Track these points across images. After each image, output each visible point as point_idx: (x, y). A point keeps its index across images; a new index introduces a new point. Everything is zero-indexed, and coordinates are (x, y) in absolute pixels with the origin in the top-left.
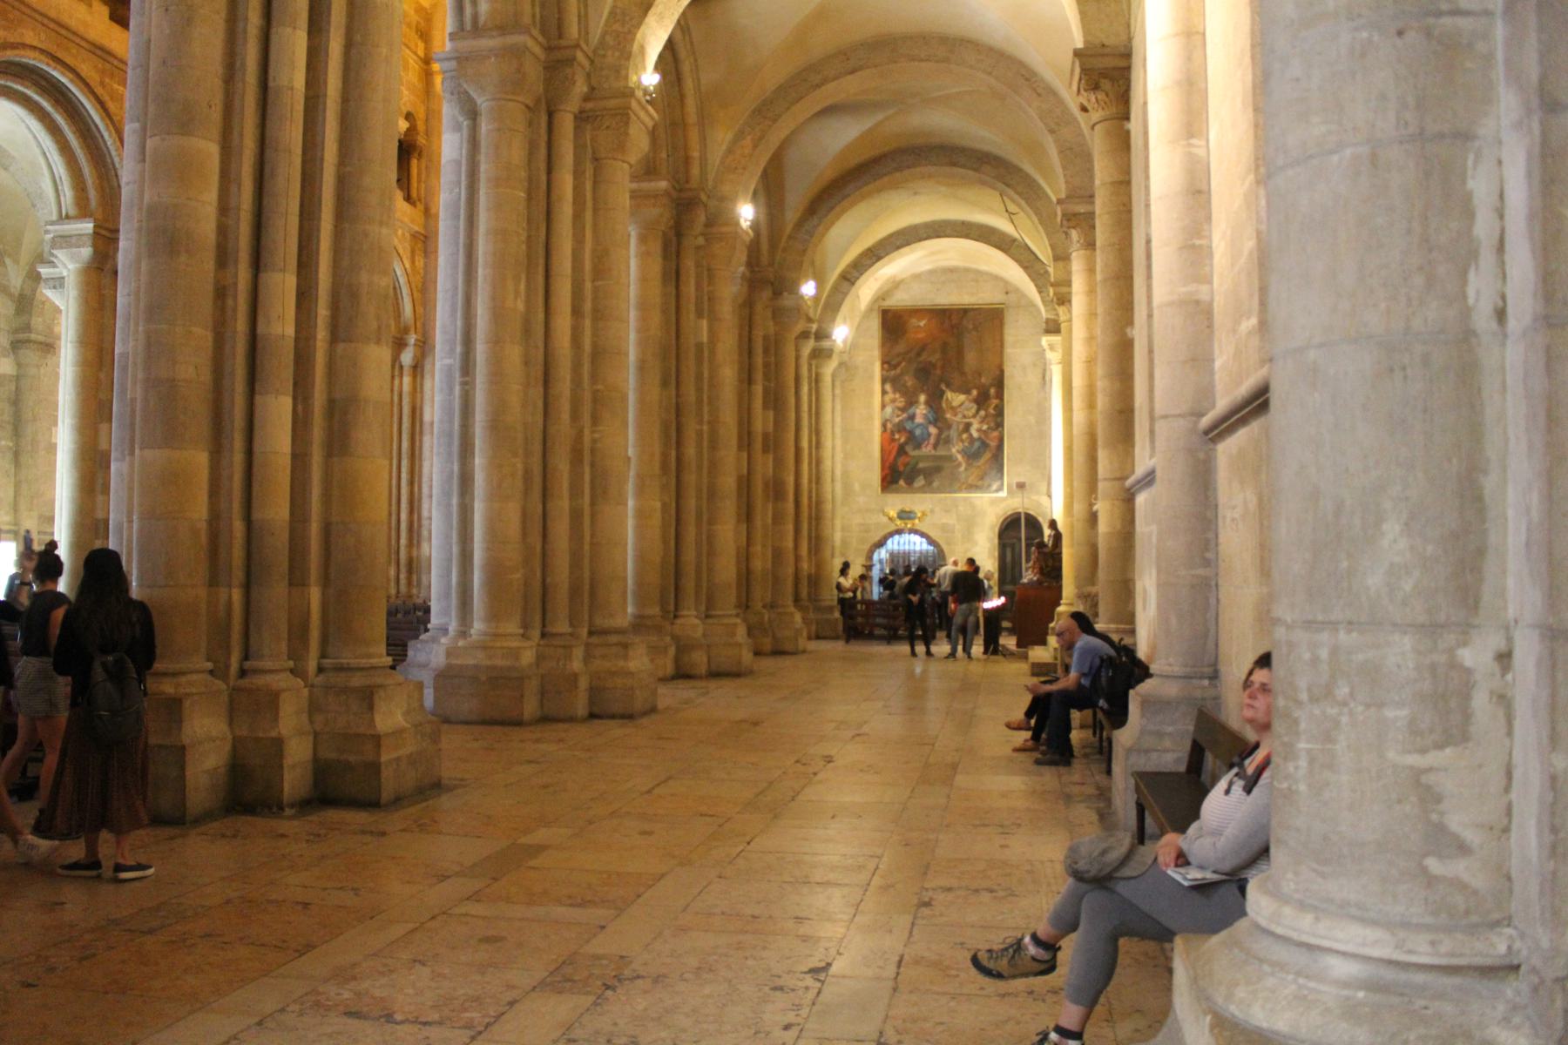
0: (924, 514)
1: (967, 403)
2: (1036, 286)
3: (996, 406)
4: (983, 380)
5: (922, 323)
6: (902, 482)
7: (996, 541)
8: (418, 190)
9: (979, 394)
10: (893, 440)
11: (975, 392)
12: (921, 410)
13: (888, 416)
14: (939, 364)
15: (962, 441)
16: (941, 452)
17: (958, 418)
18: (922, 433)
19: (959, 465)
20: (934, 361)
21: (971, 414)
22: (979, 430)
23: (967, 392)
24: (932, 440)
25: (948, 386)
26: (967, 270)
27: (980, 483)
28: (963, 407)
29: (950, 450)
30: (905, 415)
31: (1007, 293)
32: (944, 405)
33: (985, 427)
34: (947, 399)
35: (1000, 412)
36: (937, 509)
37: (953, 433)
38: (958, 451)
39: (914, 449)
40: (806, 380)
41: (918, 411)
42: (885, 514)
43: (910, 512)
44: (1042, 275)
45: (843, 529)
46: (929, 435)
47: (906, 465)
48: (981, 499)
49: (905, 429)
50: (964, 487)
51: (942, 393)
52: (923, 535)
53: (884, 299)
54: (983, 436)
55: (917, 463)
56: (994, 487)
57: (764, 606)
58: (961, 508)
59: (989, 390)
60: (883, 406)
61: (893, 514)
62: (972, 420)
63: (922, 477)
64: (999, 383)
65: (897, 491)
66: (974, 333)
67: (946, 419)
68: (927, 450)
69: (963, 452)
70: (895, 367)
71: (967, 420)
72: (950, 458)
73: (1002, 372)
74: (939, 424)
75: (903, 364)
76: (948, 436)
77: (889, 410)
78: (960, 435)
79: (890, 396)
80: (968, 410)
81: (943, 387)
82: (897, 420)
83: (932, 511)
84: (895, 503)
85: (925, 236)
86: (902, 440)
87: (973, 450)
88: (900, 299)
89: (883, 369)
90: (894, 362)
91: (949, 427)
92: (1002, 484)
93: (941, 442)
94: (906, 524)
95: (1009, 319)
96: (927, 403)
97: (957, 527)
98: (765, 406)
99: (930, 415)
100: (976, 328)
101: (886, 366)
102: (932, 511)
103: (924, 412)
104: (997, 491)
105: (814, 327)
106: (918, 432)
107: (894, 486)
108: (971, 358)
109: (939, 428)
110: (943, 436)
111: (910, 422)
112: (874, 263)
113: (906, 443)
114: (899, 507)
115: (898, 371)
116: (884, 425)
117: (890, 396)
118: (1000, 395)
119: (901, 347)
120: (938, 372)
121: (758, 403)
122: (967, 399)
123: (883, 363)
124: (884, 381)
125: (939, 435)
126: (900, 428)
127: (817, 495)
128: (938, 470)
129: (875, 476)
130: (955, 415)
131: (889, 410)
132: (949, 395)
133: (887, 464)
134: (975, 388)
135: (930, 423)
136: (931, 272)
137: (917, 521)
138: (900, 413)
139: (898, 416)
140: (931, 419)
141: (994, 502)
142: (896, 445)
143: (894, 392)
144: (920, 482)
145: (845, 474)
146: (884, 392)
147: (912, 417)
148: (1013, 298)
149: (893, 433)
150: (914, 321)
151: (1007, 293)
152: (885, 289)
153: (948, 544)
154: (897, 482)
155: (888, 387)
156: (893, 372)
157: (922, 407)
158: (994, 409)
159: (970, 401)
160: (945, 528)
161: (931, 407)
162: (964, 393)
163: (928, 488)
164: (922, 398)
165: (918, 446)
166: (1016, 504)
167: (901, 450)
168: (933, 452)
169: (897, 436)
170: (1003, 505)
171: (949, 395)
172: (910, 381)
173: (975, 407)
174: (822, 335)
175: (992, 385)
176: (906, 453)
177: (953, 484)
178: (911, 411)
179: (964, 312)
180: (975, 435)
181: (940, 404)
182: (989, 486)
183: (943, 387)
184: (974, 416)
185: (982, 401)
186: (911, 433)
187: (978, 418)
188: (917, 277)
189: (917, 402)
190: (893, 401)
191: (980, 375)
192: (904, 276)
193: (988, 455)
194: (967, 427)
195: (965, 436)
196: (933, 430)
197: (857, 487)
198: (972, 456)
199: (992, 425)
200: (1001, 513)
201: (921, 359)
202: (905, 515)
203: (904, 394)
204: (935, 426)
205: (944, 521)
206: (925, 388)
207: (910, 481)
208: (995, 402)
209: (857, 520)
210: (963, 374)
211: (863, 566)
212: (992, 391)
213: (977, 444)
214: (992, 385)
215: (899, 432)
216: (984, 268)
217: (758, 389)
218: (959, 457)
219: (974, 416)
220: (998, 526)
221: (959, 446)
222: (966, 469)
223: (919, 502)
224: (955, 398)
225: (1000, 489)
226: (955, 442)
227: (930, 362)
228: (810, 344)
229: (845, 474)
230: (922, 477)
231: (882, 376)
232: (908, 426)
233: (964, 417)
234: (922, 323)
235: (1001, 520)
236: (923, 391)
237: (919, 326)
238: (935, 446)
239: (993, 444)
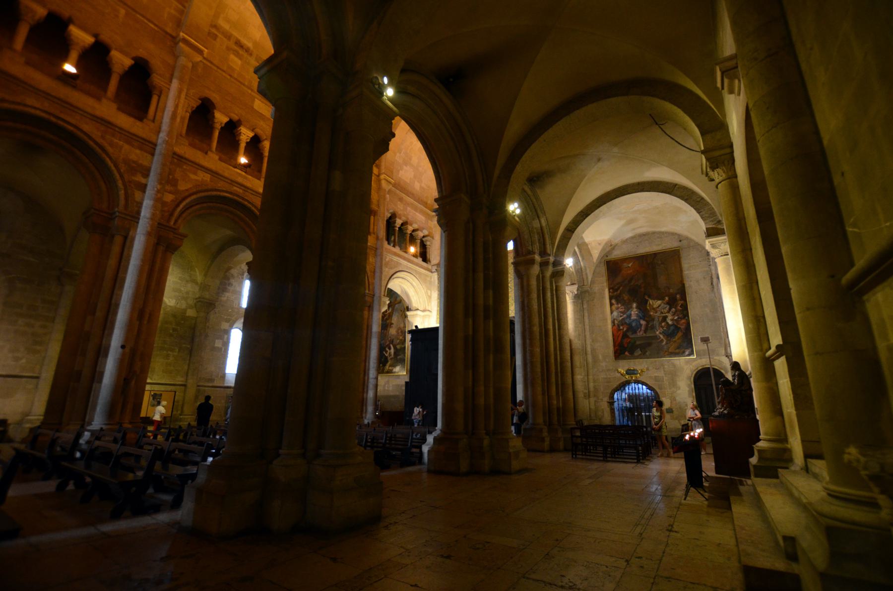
0: (642, 371)
1: (662, 305)
2: (695, 209)
3: (682, 305)
4: (671, 291)
5: (630, 265)
6: (627, 353)
7: (693, 386)
8: (374, 229)
9: (669, 299)
10: (620, 330)
11: (667, 298)
12: (634, 312)
13: (615, 317)
15: (662, 327)
17: (658, 314)
18: (637, 324)
19: (662, 340)
21: (666, 311)
22: (672, 320)
23: (662, 299)
24: (643, 328)
25: (649, 297)
26: (654, 233)
27: (677, 351)
28: (660, 308)
29: (656, 333)
30: (625, 316)
31: (680, 241)
32: (648, 308)
33: (676, 318)
34: (650, 304)
35: (685, 308)
36: (650, 368)
37: (656, 323)
38: (660, 333)
39: (632, 334)
40: (549, 290)
41: (633, 312)
42: (619, 372)
43: (634, 370)
44: (699, 202)
45: (594, 381)
46: (641, 325)
48: (681, 361)
49: (626, 323)
50: (667, 353)
51: (647, 301)
52: (643, 384)
53: (607, 256)
54: (675, 324)
55: (635, 342)
56: (687, 353)
57: (487, 434)
58: (666, 367)
59: (676, 297)
60: (612, 313)
61: (623, 371)
62: (667, 314)
63: (639, 349)
65: (624, 359)
66: (662, 265)
67: (651, 315)
68: (640, 334)
69: (663, 333)
70: (617, 290)
71: (664, 315)
72: (656, 337)
73: (683, 285)
74: (646, 319)
75: (621, 288)
76: (653, 325)
77: (615, 314)
78: (660, 323)
79: (616, 306)
80: (663, 309)
82: (621, 318)
83: (648, 369)
84: (623, 366)
85: (615, 197)
86: (625, 329)
87: (670, 331)
88: (617, 254)
89: (609, 292)
90: (616, 288)
91: (653, 320)
92: (692, 351)
93: (649, 328)
94: (632, 377)
95: (683, 255)
96: (637, 308)
97: (665, 378)
98: (486, 288)
99: (640, 315)
101: (611, 290)
102: (648, 369)
103: (636, 312)
104: (689, 355)
105: (552, 259)
106: (634, 324)
107: (622, 356)
108: (662, 280)
109: (646, 321)
110: (649, 325)
111: (628, 319)
112: (585, 219)
113: (627, 330)
114: (626, 368)
115: (619, 292)
116: (613, 322)
117: (614, 307)
118: (684, 297)
119: (619, 279)
120: (642, 290)
121: (481, 284)
123: (609, 290)
124: (611, 299)
125: (647, 325)
126: (622, 322)
127: (561, 358)
128: (649, 344)
129: (611, 350)
130: (656, 312)
131: (615, 314)
132: (651, 301)
133: (617, 343)
134: (666, 296)
135: (641, 318)
136: (632, 238)
137: (638, 375)
138: (622, 315)
139: (621, 316)
140: (641, 316)
141: (688, 362)
142: (621, 333)
143: (618, 304)
144: (638, 352)
145: (593, 350)
146: (611, 305)
147: (629, 316)
148: (685, 243)
149: (618, 325)
150: (625, 265)
151: (680, 241)
152: (608, 250)
153: (660, 389)
154: (624, 353)
155: (613, 301)
156: (615, 293)
157: (635, 310)
158: (680, 306)
159: (664, 303)
160: (656, 379)
161: (640, 310)
162: (660, 300)
163: (643, 356)
164: (634, 305)
165: (635, 332)
166: (704, 362)
167: (625, 335)
168: (644, 335)
169: (621, 328)
170: (694, 364)
172: (626, 297)
173: (668, 307)
174: (558, 263)
176: (628, 337)
177: (659, 353)
178: (628, 313)
179: (655, 255)
180: (670, 323)
182: (684, 352)
184: (668, 312)
185: (672, 303)
186: (630, 325)
187: (671, 312)
188: (625, 242)
189: (631, 307)
190: (617, 308)
192: (616, 241)
193: (680, 334)
194: (665, 318)
195: (663, 324)
196: (643, 322)
197: (600, 357)
198: (669, 335)
199: (681, 316)
200: (694, 369)
201: (632, 284)
202: (630, 372)
203: (623, 305)
204: (644, 320)
205: (656, 375)
206: (635, 300)
207: (632, 352)
209: (602, 376)
211: (608, 402)
213: (672, 328)
215: (622, 325)
216: (663, 229)
217: (481, 276)
218: (661, 336)
220: (693, 376)
222: (667, 344)
223: (639, 364)
224: (656, 303)
225: (692, 353)
226: (657, 328)
228: (550, 270)
229: (593, 350)
230: (639, 349)
231: (610, 296)
232: (627, 321)
233: (662, 313)
234: (630, 265)
235: (695, 373)
236: (634, 301)
237: (629, 267)
238: (645, 332)
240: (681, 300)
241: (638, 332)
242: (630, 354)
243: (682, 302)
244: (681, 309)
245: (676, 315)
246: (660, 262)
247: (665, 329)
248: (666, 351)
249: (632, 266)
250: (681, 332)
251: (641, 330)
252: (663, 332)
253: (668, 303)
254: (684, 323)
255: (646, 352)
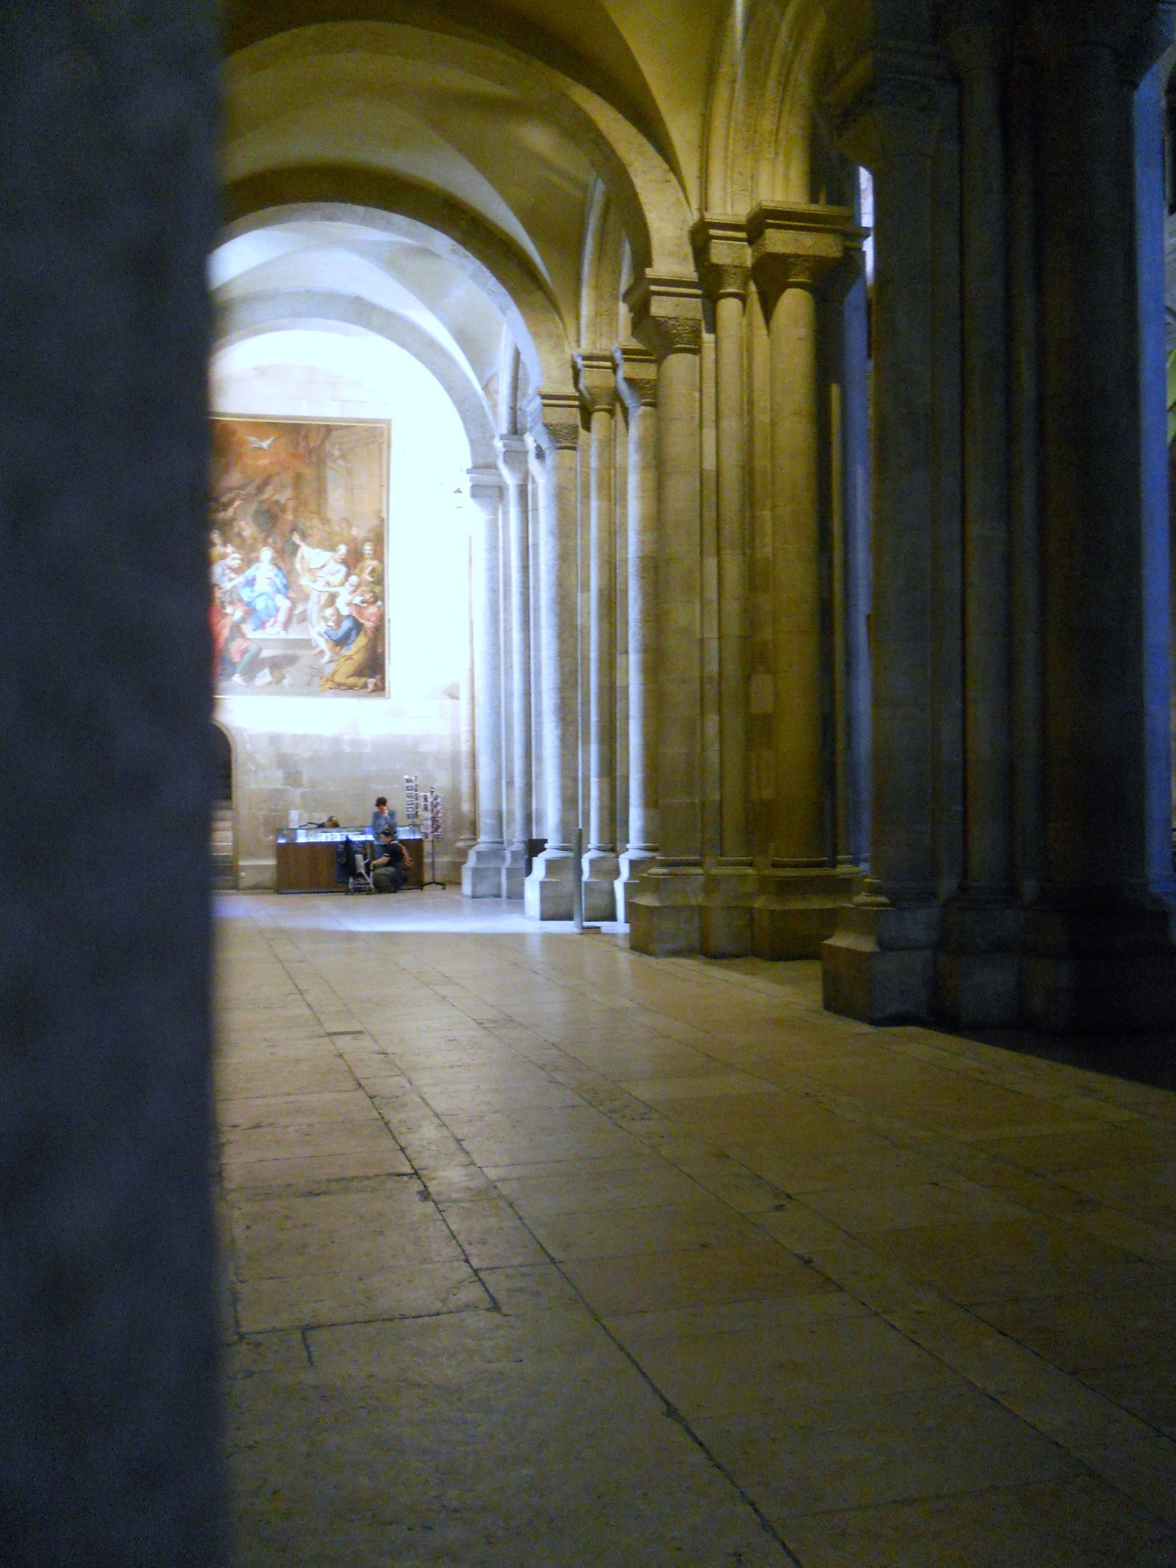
3: (373, 571)
4: (355, 532)
9: (349, 551)
11: (343, 549)
14: (291, 505)
15: (325, 619)
16: (294, 634)
18: (267, 607)
19: (322, 652)
20: (283, 501)
23: (332, 548)
24: (282, 616)
25: (304, 537)
28: (324, 570)
32: (298, 566)
33: (357, 600)
35: (379, 579)
37: (312, 607)
38: (320, 635)
47: (244, 652)
51: (296, 547)
55: (259, 651)
62: (339, 589)
64: (379, 539)
66: (340, 462)
67: (301, 586)
68: (274, 631)
74: (291, 594)
76: (305, 611)
81: (296, 538)
91: (306, 598)
93: (295, 619)
100: (343, 456)
106: (260, 604)
108: (336, 500)
113: (243, 620)
118: (379, 555)
120: (289, 517)
122: (332, 557)
125: (291, 610)
130: (315, 581)
132: (305, 550)
135: (278, 591)
140: (280, 586)
150: (253, 441)
165: (262, 625)
171: (305, 550)
175: (368, 540)
176: (243, 636)
178: (250, 573)
180: (345, 611)
181: (292, 563)
183: (296, 538)
185: (353, 561)
187: (347, 585)
191: (349, 524)
194: (332, 599)
195: (329, 612)
199: (368, 596)
201: (264, 497)
208: (370, 564)
210: (326, 521)
212: (368, 548)
213: (347, 625)
214: (368, 540)
219: (342, 584)
221: (322, 627)
227: (277, 502)
230: (267, 671)
233: (328, 584)
234: (265, 444)
236: (265, 544)
237: (261, 448)
238: (286, 625)
239: (369, 625)
240: (372, 559)
241: (268, 624)
242: (245, 680)
243: (374, 563)
244: (371, 579)
245: (359, 591)
246: (336, 453)
247: (332, 624)
248: (327, 680)
249: (270, 446)
250: (365, 635)
251: (275, 622)
252: (326, 633)
253: (344, 562)
254: (372, 614)
255: (284, 677)
